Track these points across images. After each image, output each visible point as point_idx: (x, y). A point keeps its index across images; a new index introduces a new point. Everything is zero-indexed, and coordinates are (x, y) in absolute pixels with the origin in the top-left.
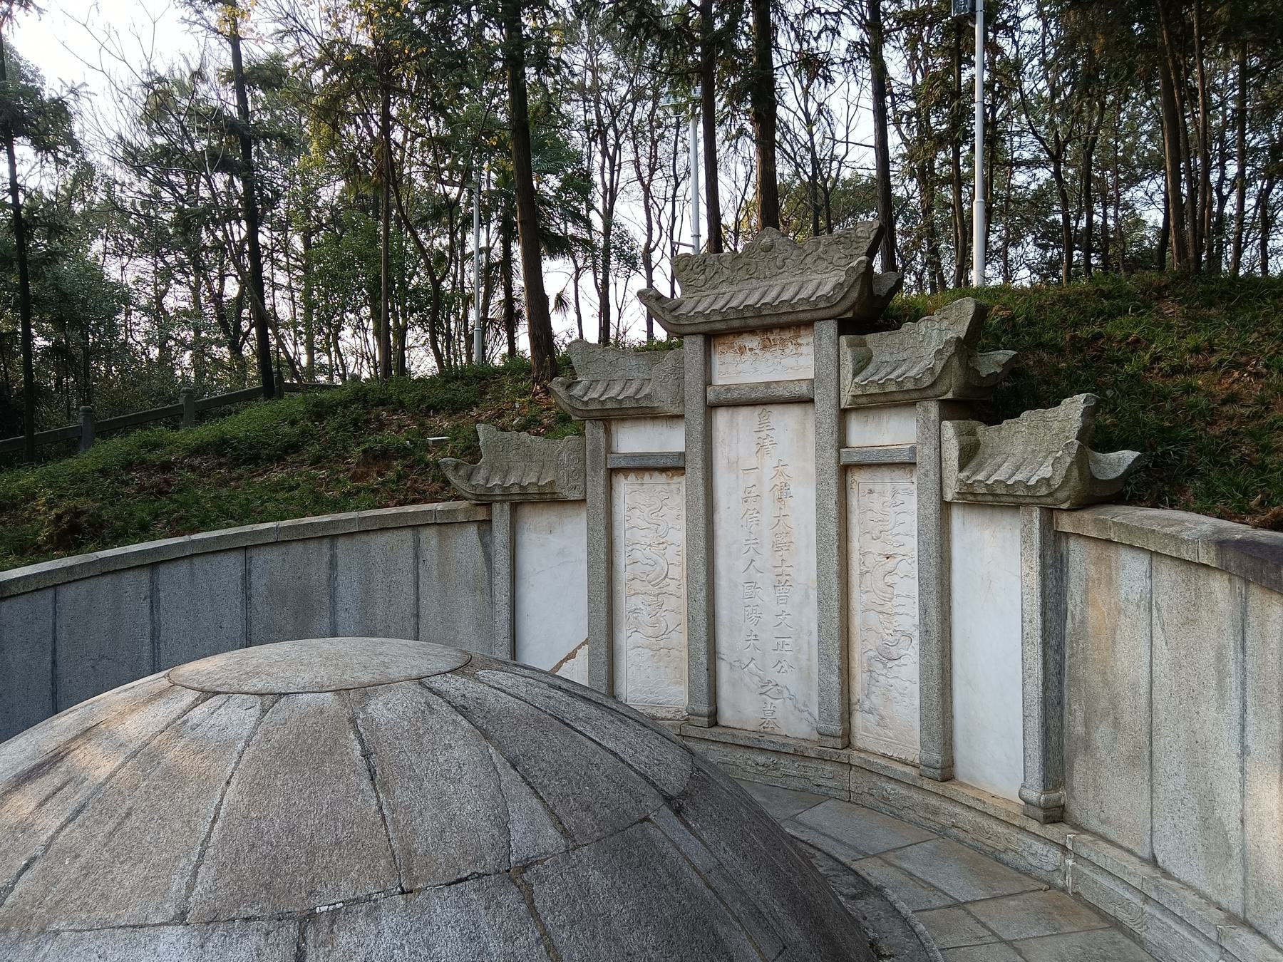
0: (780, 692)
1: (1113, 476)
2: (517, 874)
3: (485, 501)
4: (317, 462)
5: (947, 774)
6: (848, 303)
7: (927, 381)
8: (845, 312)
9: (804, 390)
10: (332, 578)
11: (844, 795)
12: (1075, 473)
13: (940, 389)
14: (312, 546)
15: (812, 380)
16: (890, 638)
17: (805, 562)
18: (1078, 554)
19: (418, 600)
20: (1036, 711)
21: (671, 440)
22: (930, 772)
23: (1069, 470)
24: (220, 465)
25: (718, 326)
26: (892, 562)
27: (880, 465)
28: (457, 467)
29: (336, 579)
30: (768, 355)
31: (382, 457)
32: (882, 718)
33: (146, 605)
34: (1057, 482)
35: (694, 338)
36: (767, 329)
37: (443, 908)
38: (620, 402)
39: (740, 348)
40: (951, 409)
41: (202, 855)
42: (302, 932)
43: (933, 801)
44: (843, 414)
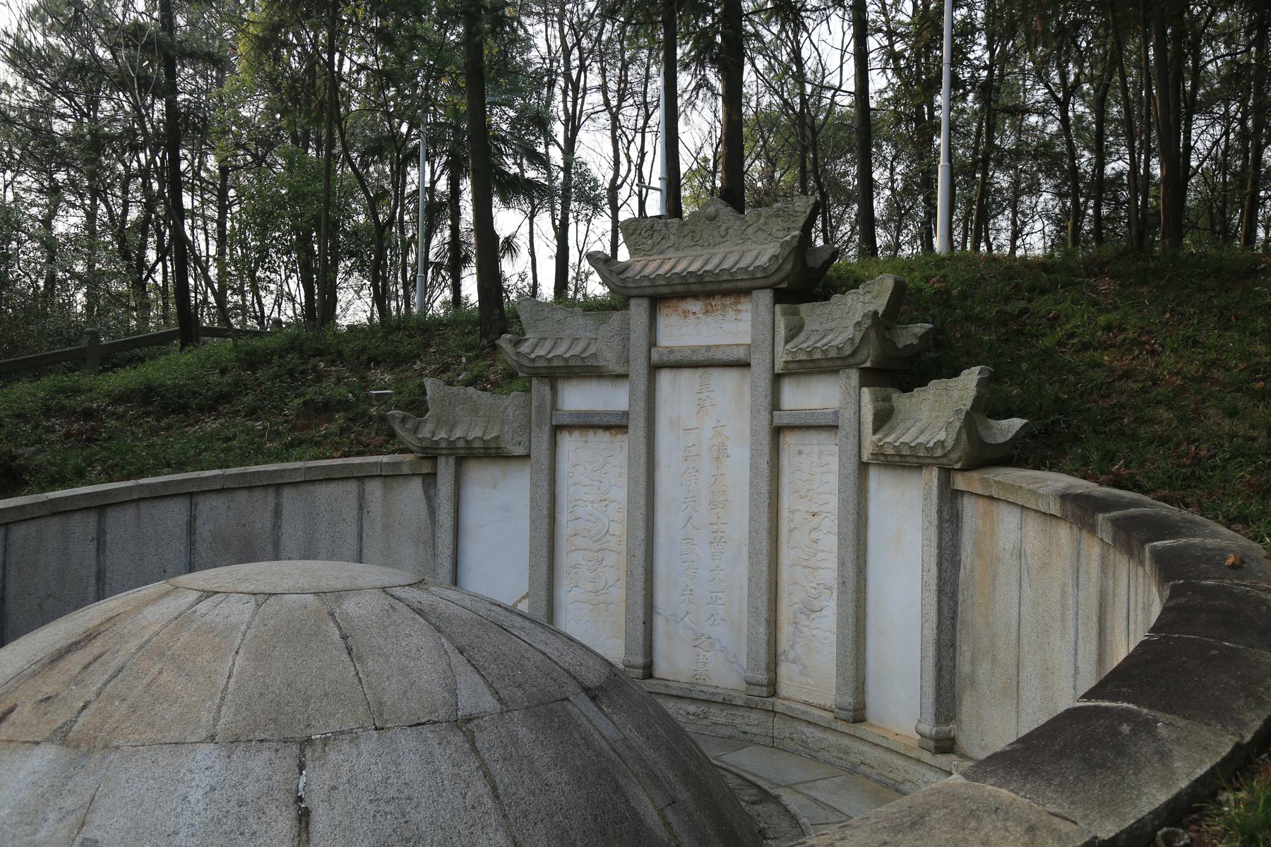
0: (712, 645)
1: (1001, 440)
2: (464, 724)
3: (431, 454)
4: (252, 413)
5: (858, 715)
6: (782, 274)
7: (848, 350)
8: (780, 282)
9: (740, 354)
10: (276, 527)
11: (768, 740)
12: (964, 437)
13: (859, 358)
14: (258, 494)
15: (749, 345)
16: (814, 591)
17: (739, 519)
18: (970, 508)
19: (361, 550)
20: (931, 652)
22: (844, 714)
23: (959, 433)
24: (148, 414)
25: (663, 290)
26: (817, 519)
27: (808, 427)
28: (404, 420)
29: (279, 527)
30: (710, 319)
31: (325, 409)
32: (805, 667)
33: (92, 547)
34: (949, 444)
35: (640, 301)
36: (709, 295)
37: (407, 741)
38: (567, 360)
39: (684, 312)
40: (870, 377)
41: (223, 699)
42: (302, 750)
43: (846, 741)
44: (777, 379)
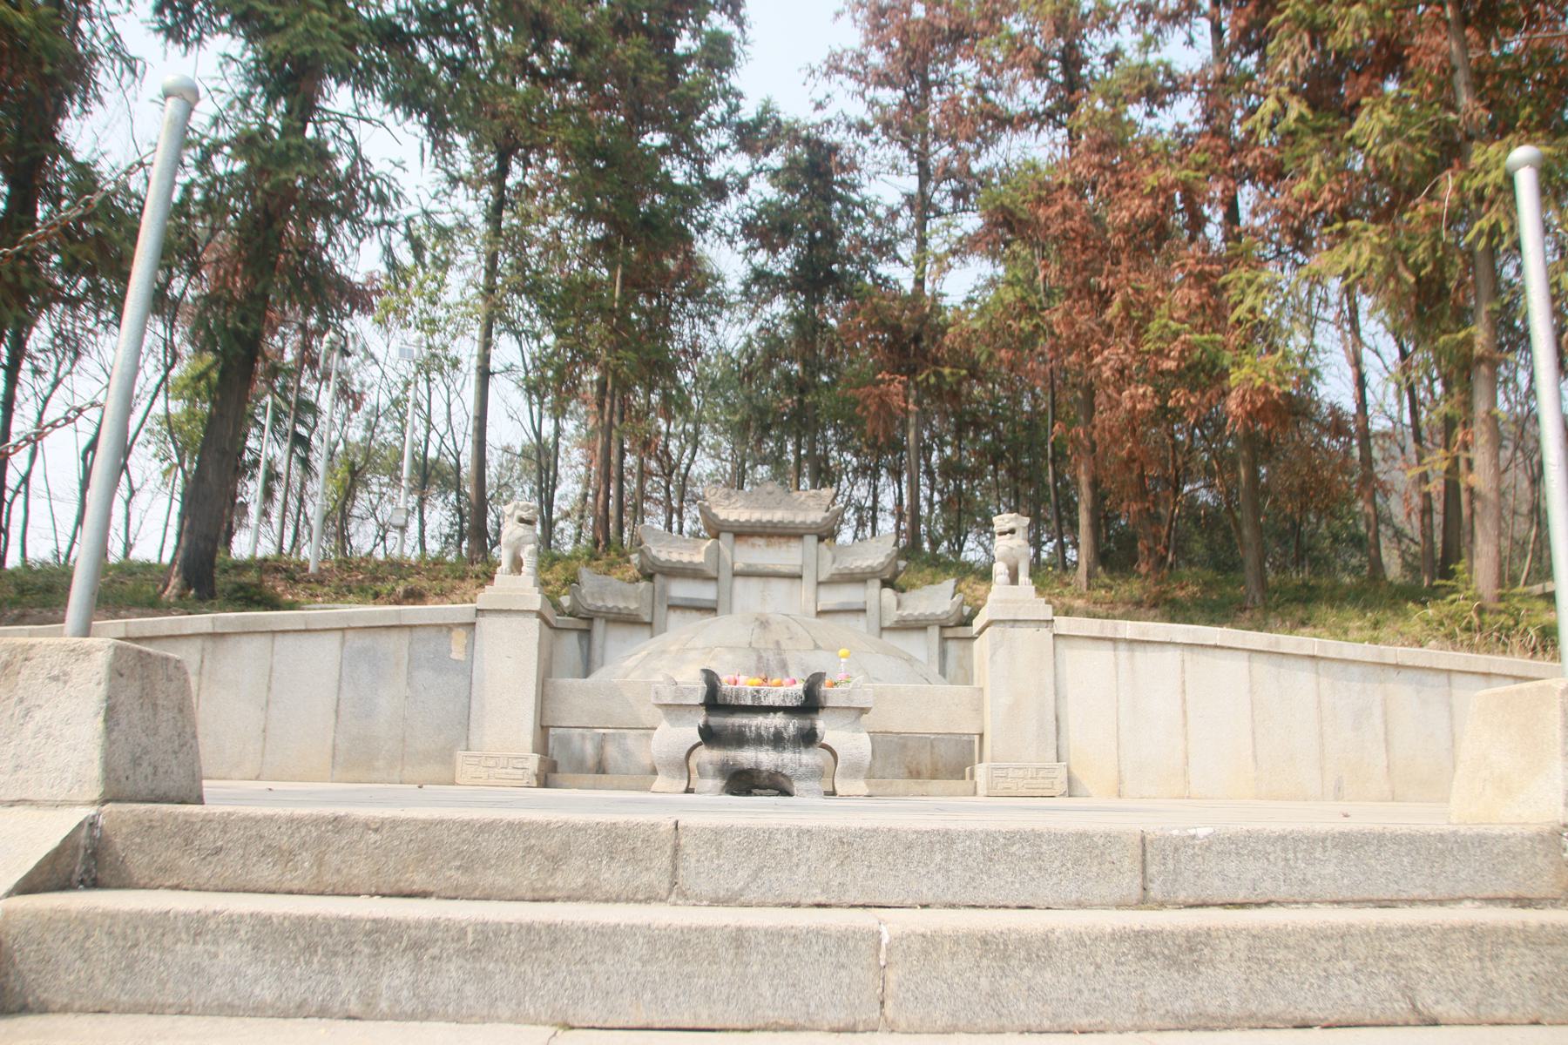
9: (797, 570)
21: (705, 592)
